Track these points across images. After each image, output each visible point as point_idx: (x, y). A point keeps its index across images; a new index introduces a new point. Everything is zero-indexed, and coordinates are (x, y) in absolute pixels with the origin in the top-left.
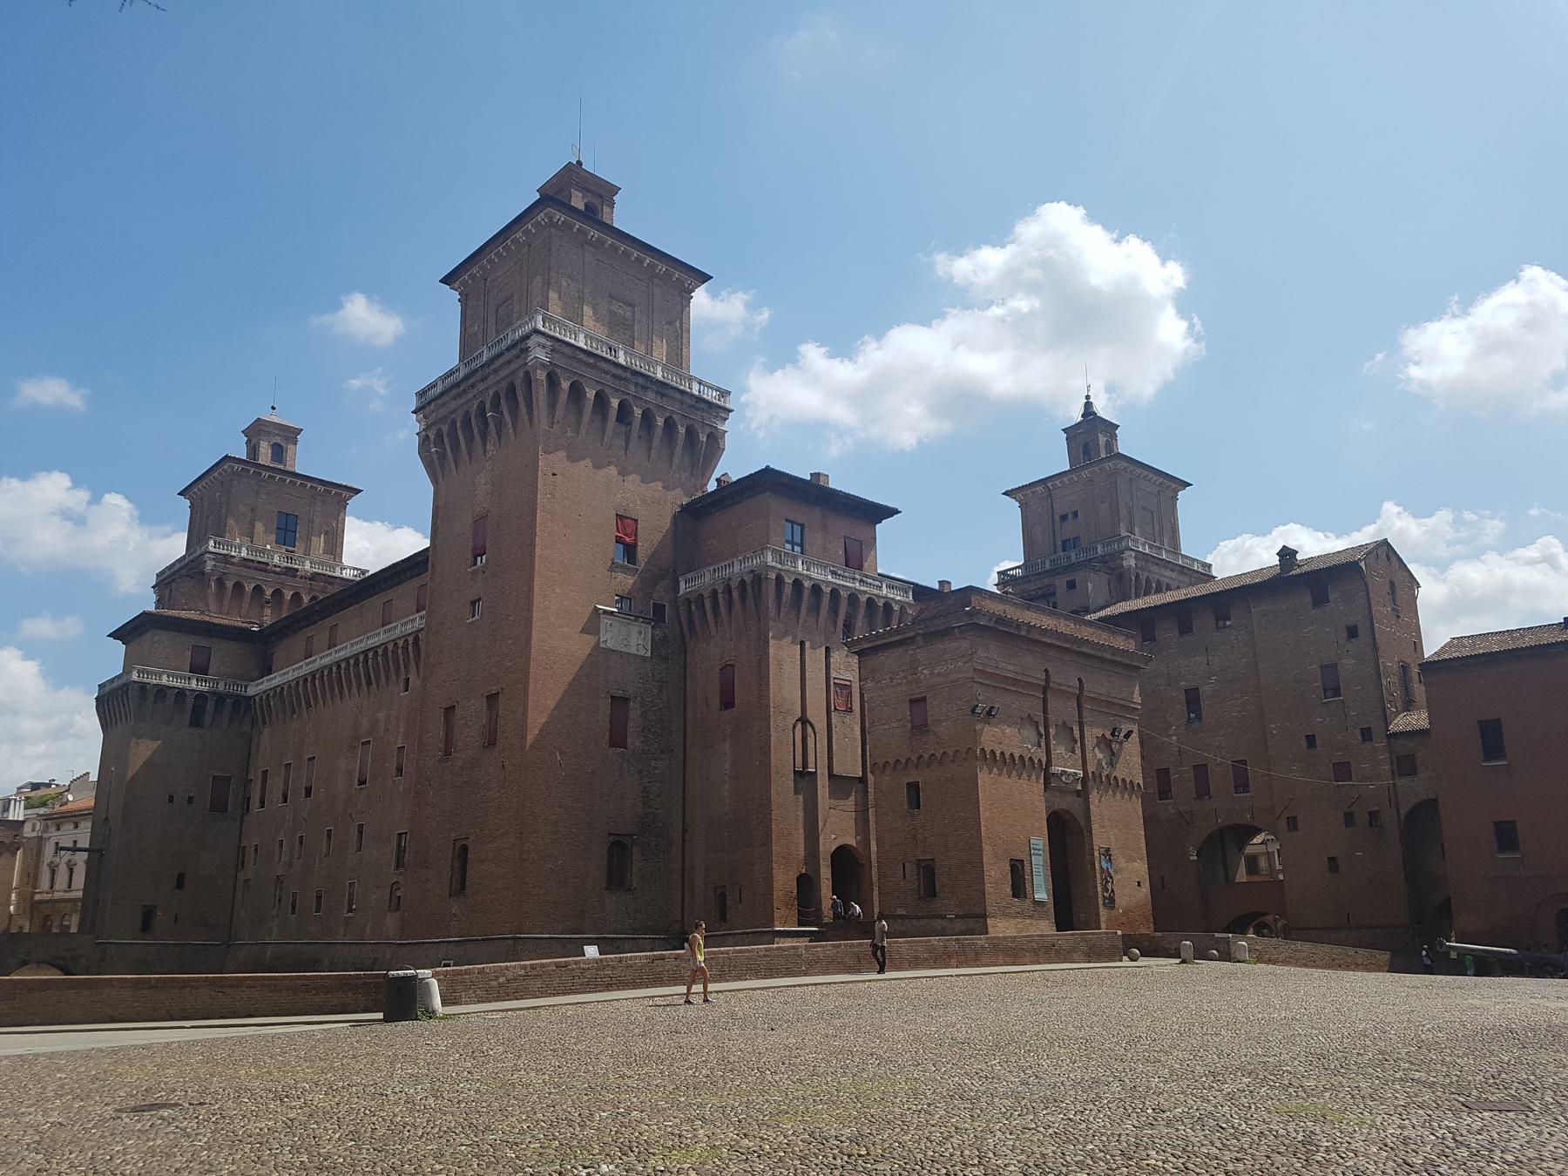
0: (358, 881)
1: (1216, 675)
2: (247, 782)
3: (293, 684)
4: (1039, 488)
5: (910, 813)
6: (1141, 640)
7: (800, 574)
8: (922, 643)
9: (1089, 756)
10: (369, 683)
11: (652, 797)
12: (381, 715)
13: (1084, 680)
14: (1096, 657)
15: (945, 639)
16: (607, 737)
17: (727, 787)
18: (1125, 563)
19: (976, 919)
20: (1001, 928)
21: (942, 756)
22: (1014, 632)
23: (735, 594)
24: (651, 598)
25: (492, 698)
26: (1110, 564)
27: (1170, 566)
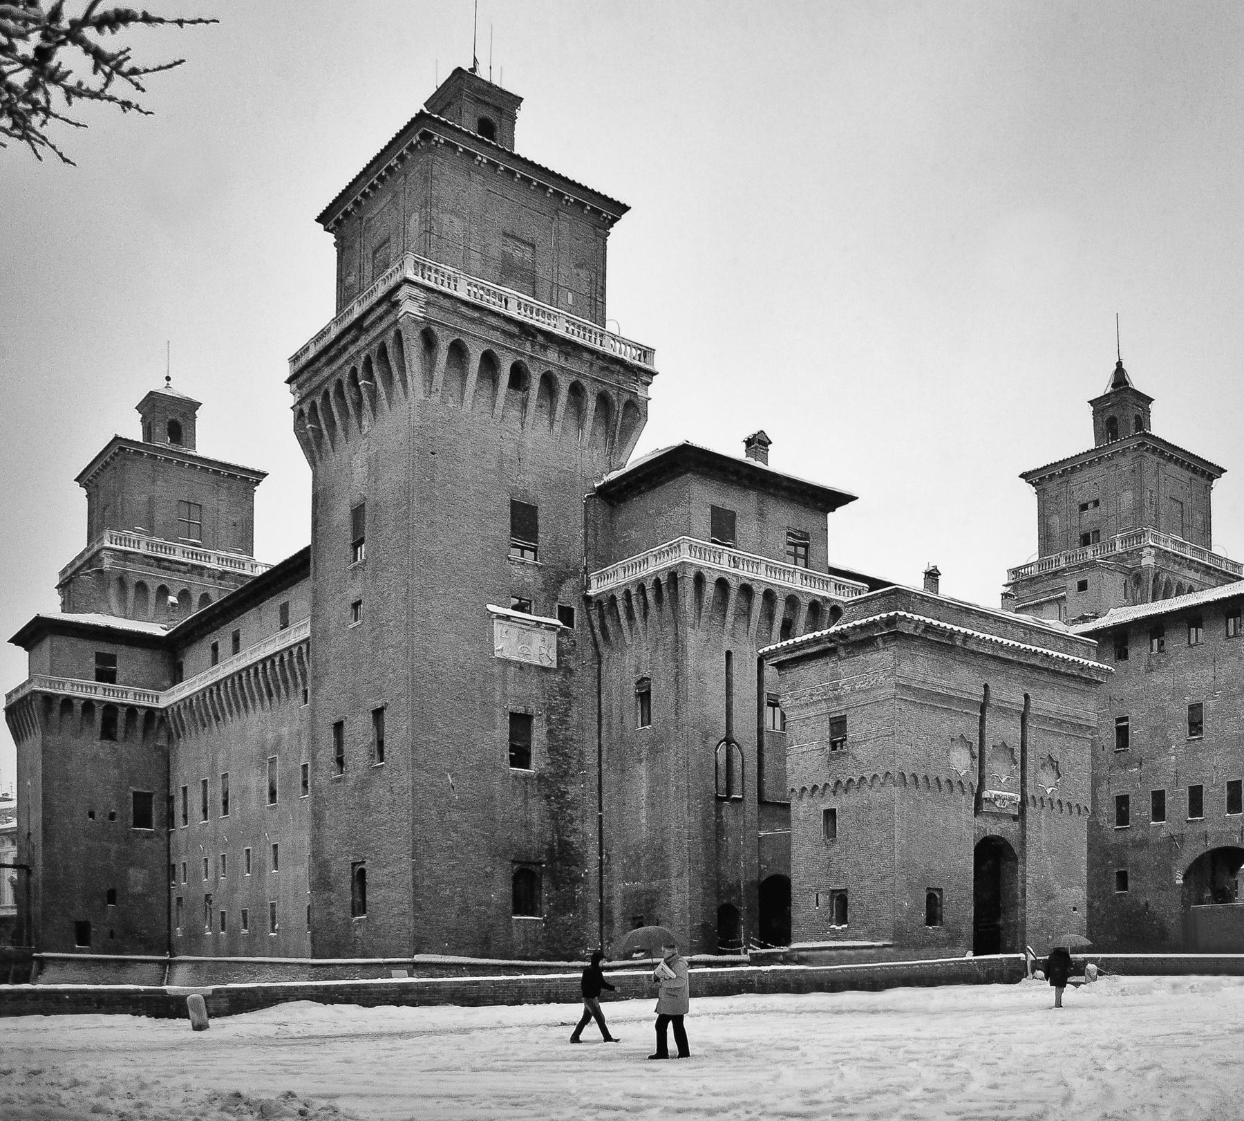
9: (1029, 781)
14: (1047, 670)
21: (860, 781)
22: (947, 642)
23: (650, 596)
24: (556, 599)
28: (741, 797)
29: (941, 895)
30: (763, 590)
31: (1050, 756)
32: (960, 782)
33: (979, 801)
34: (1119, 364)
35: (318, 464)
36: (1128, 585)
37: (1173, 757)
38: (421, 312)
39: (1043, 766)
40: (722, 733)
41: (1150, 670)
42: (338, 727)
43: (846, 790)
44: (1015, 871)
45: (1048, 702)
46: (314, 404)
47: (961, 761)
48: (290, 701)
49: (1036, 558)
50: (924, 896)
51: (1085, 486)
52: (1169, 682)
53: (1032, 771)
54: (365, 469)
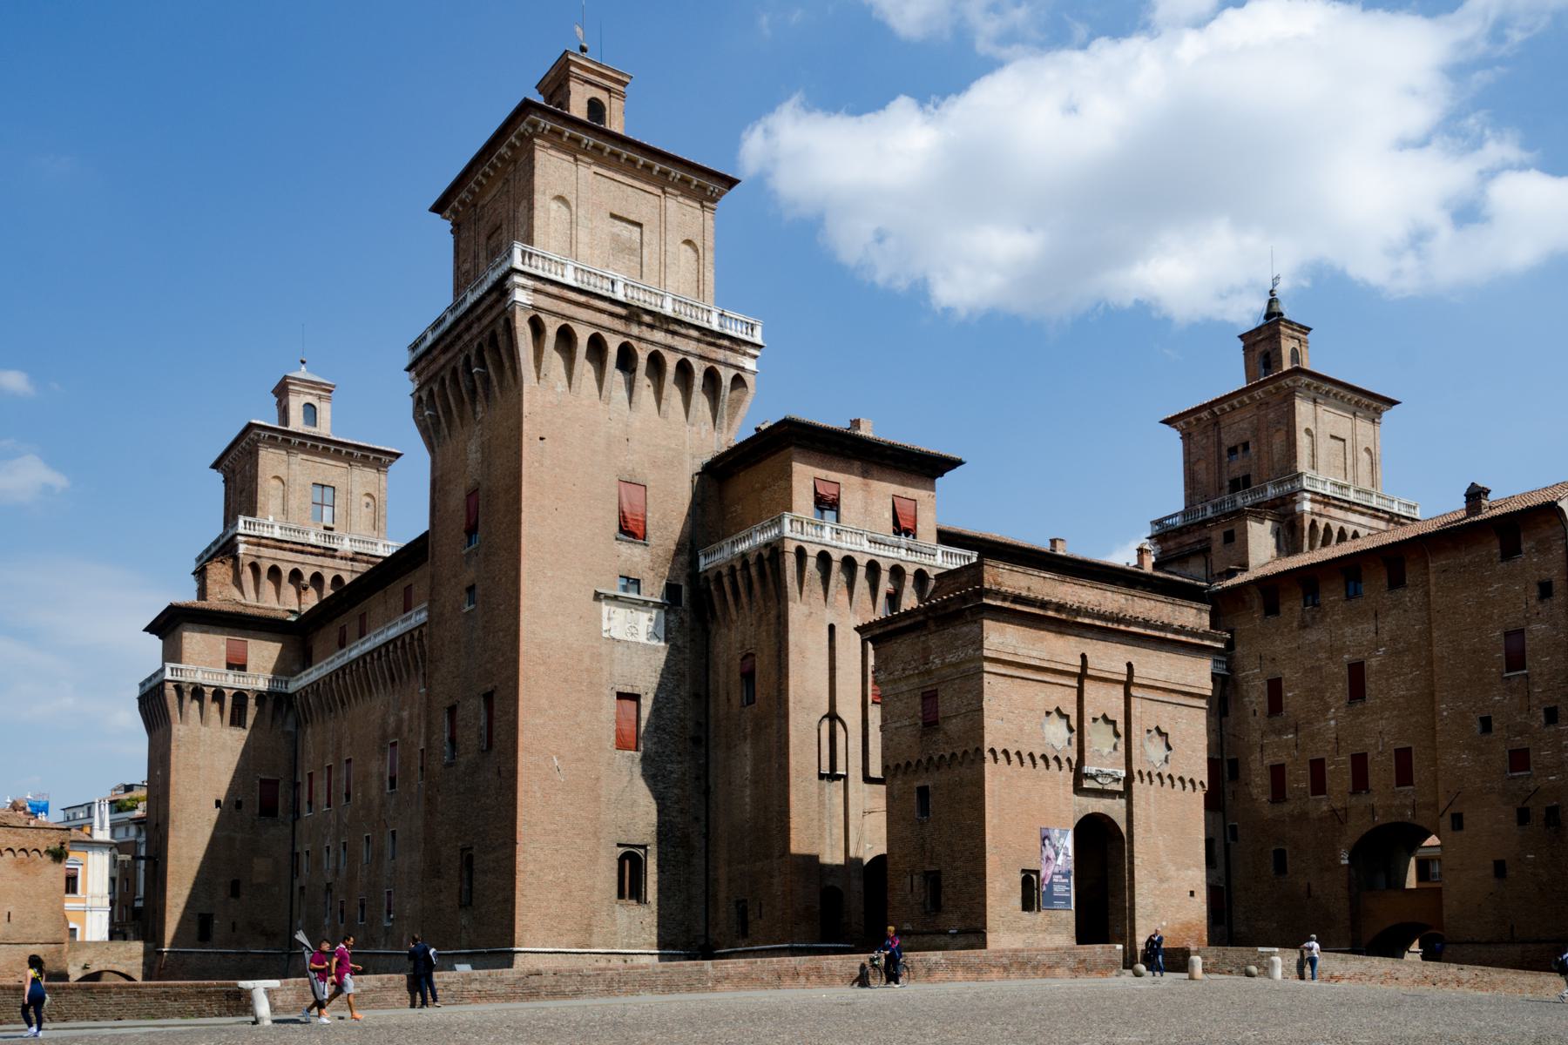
0: (394, 890)
1: (1385, 645)
2: (296, 785)
3: (327, 679)
4: (1205, 415)
5: (919, 820)
6: (1302, 605)
7: (826, 545)
8: (933, 628)
9: (1135, 752)
10: (393, 680)
11: (669, 804)
12: (405, 714)
15: (957, 623)
16: (613, 738)
17: (748, 792)
19: (975, 934)
23: (753, 571)
25: (488, 697)
30: (865, 562)
31: (1158, 729)
33: (1079, 776)
35: (436, 450)
37: (1332, 722)
38: (528, 299)
39: (1152, 737)
41: (1304, 626)
42: (452, 711)
46: (431, 391)
47: (1057, 735)
48: (411, 685)
50: (1019, 877)
52: (1325, 639)
53: (1138, 744)
54: (479, 455)
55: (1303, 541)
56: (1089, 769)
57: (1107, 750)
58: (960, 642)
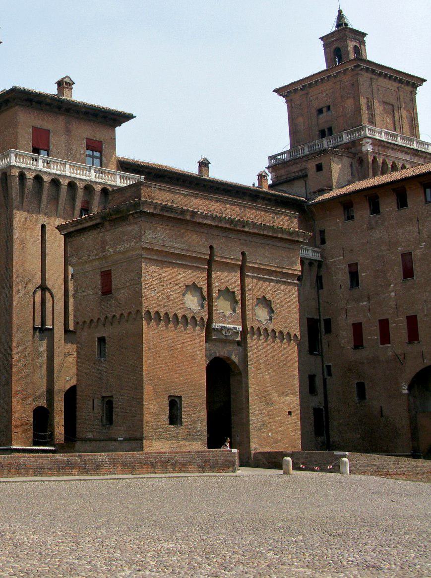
8: (108, 227)
9: (249, 314)
13: (247, 253)
14: (258, 234)
18: (364, 149)
19: (136, 440)
20: (154, 446)
22: (179, 217)
26: (353, 151)
27: (405, 150)
28: (51, 327)
29: (181, 400)
32: (193, 317)
34: (340, 12)
36: (354, 166)
40: (38, 282)
41: (371, 228)
43: (128, 320)
44: (240, 382)
45: (259, 257)
49: (288, 148)
51: (319, 97)
53: (251, 308)
55: (368, 171)
56: (216, 325)
57: (228, 312)
58: (126, 237)
